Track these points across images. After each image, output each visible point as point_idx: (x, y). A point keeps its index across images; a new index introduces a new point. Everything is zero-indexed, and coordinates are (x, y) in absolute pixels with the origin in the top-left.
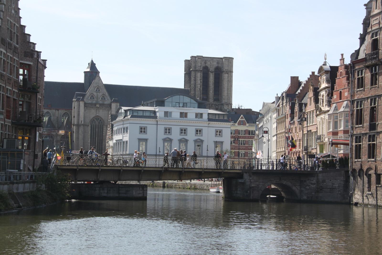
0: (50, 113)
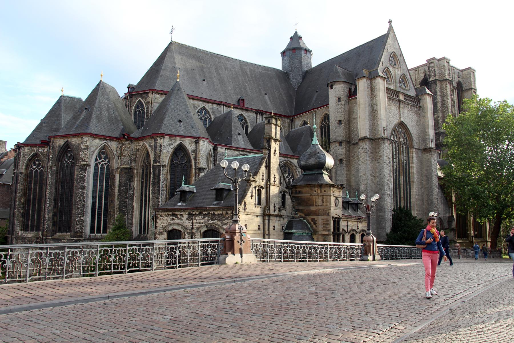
0: (245, 120)
